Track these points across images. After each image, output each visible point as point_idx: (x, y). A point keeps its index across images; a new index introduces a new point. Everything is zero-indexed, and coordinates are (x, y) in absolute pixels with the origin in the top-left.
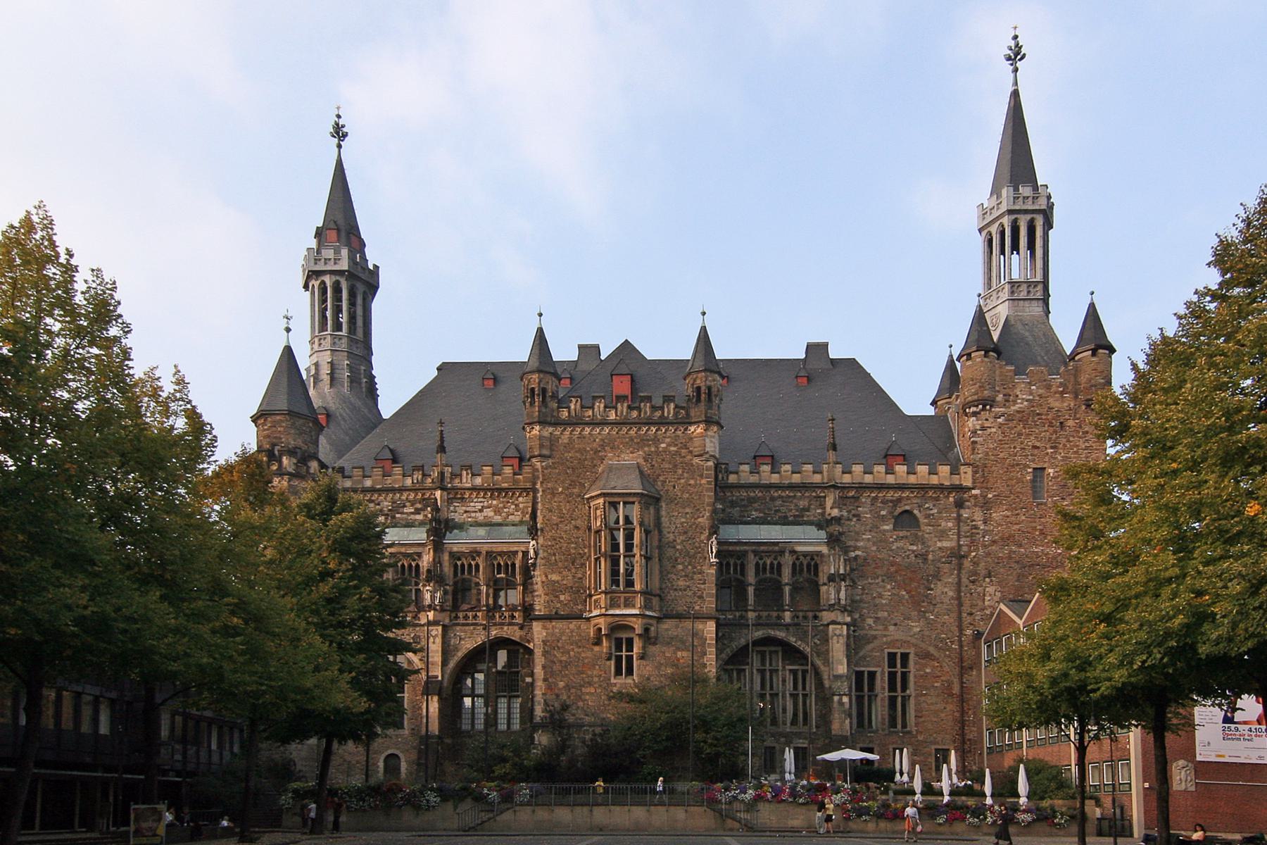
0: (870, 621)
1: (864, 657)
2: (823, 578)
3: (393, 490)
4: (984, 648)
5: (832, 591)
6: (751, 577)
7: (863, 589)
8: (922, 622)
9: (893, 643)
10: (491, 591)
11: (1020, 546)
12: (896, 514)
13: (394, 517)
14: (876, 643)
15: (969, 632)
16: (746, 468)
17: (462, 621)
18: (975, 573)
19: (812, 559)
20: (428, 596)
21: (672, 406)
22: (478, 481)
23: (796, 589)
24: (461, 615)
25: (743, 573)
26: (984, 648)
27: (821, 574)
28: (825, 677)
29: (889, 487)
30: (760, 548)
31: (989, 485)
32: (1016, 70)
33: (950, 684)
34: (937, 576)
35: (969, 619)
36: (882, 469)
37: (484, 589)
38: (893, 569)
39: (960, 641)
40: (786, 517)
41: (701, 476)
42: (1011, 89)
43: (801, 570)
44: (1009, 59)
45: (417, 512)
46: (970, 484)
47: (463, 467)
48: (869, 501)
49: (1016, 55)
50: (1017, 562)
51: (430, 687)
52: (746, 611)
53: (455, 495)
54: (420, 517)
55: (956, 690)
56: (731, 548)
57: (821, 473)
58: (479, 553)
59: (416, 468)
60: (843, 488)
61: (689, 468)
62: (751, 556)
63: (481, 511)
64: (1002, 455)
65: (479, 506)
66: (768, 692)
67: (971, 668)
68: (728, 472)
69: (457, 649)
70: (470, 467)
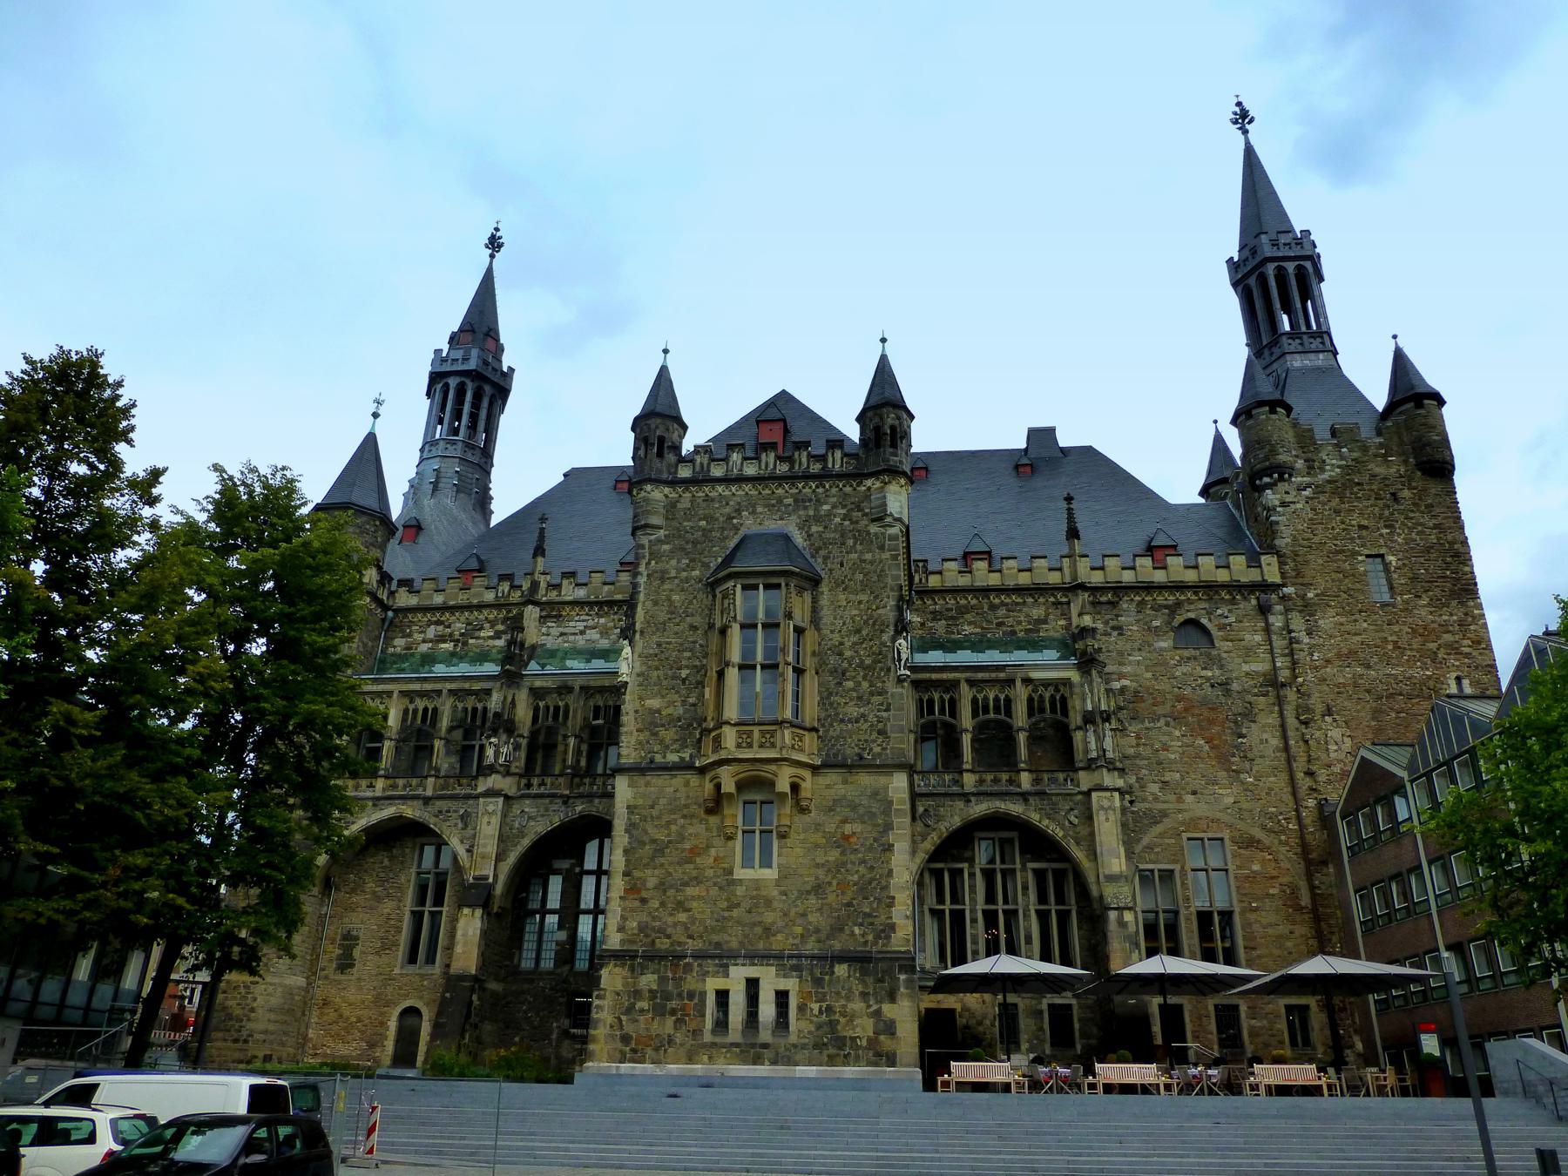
0: (1154, 788)
1: (1149, 848)
2: (1075, 719)
3: (469, 608)
4: (1342, 827)
5: (1092, 738)
6: (966, 720)
7: (1138, 737)
8: (1236, 788)
9: (1192, 824)
10: (584, 747)
11: (1368, 667)
12: (1176, 623)
13: (465, 644)
14: (1167, 823)
15: (1311, 803)
16: (953, 565)
17: (534, 791)
18: (1308, 710)
19: (1057, 690)
20: (490, 752)
21: (838, 454)
22: (581, 593)
23: (1035, 739)
24: (535, 781)
25: (953, 714)
26: (1342, 827)
27: (1071, 714)
28: (1091, 879)
29: (1161, 588)
30: (978, 677)
31: (1306, 581)
32: (1245, 132)
33: (1294, 890)
34: (1249, 715)
35: (1308, 782)
36: (1147, 562)
37: (572, 741)
38: (1180, 706)
39: (1299, 817)
40: (1014, 633)
41: (882, 548)
42: (1243, 146)
43: (1042, 710)
44: (1236, 122)
45: (497, 636)
46: (1278, 580)
47: (565, 575)
48: (1133, 607)
49: (1242, 118)
50: (1368, 691)
51: (478, 894)
52: (961, 773)
53: (553, 611)
54: (501, 643)
55: (1305, 900)
56: (934, 676)
57: (1060, 569)
58: (570, 690)
59: (502, 578)
60: (1094, 590)
61: (863, 537)
62: (964, 688)
63: (582, 633)
64: (1317, 539)
65: (581, 626)
66: (1000, 906)
67: (1325, 863)
68: (928, 573)
69: (522, 834)
70: (573, 574)
